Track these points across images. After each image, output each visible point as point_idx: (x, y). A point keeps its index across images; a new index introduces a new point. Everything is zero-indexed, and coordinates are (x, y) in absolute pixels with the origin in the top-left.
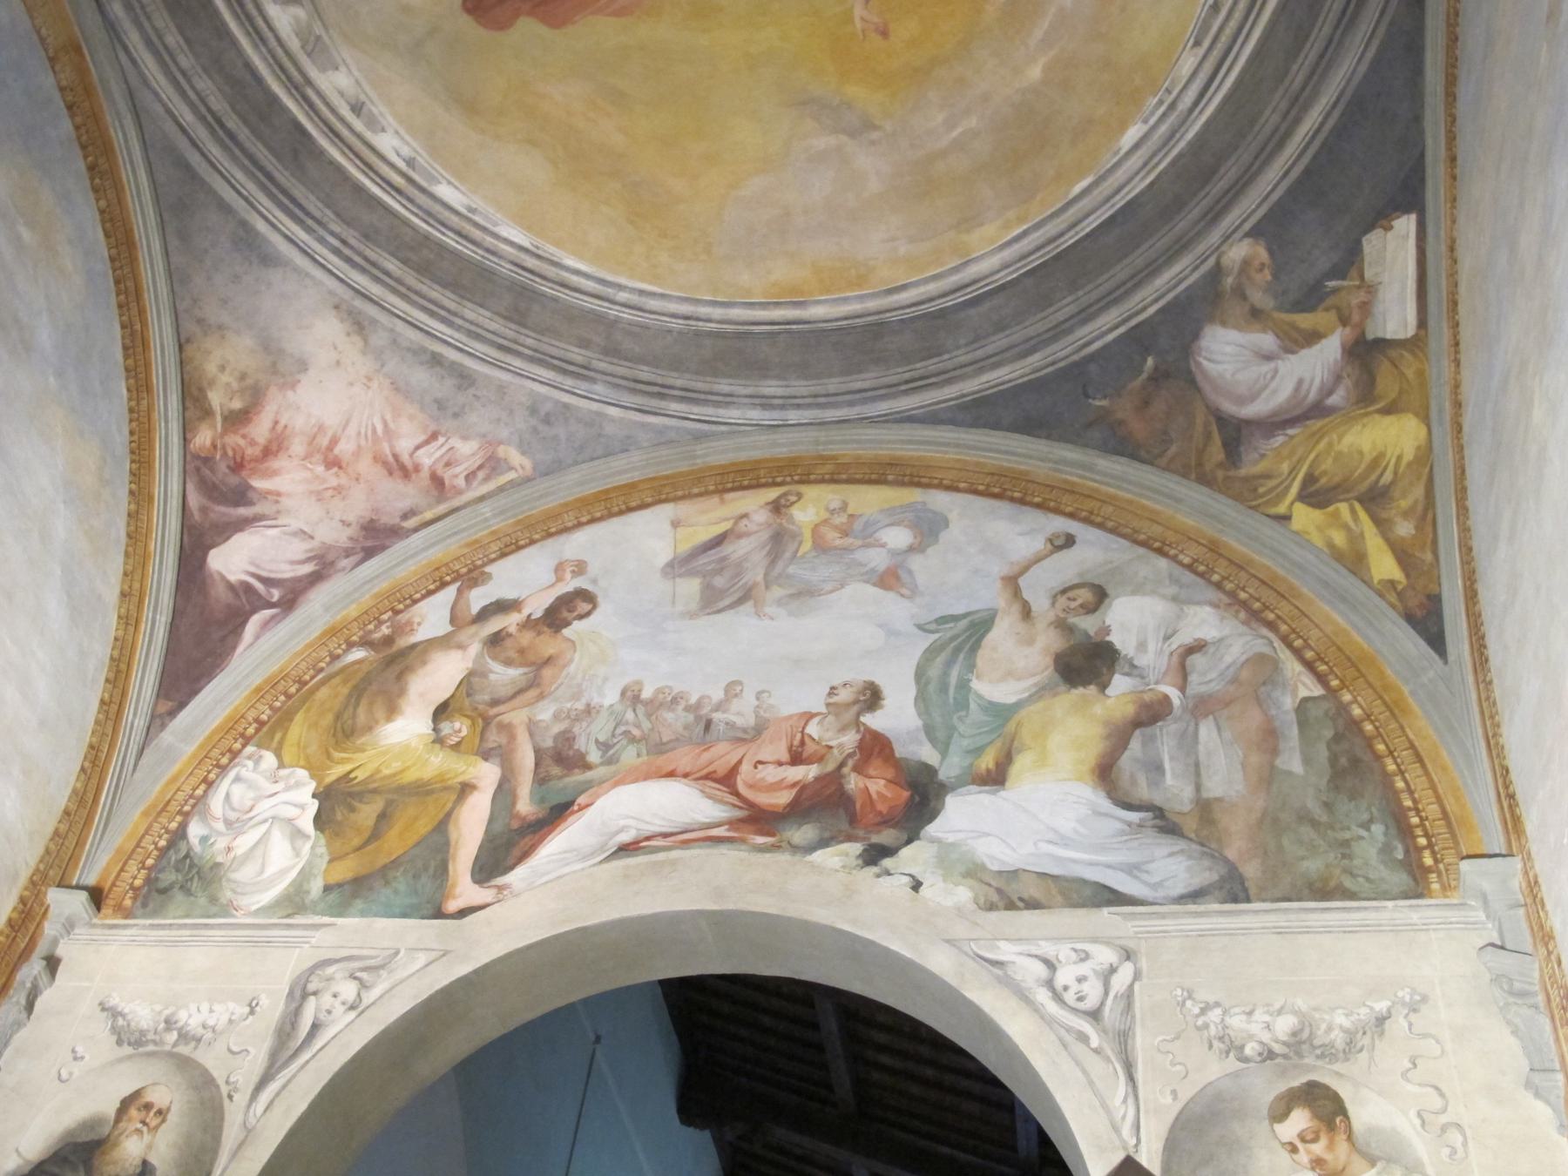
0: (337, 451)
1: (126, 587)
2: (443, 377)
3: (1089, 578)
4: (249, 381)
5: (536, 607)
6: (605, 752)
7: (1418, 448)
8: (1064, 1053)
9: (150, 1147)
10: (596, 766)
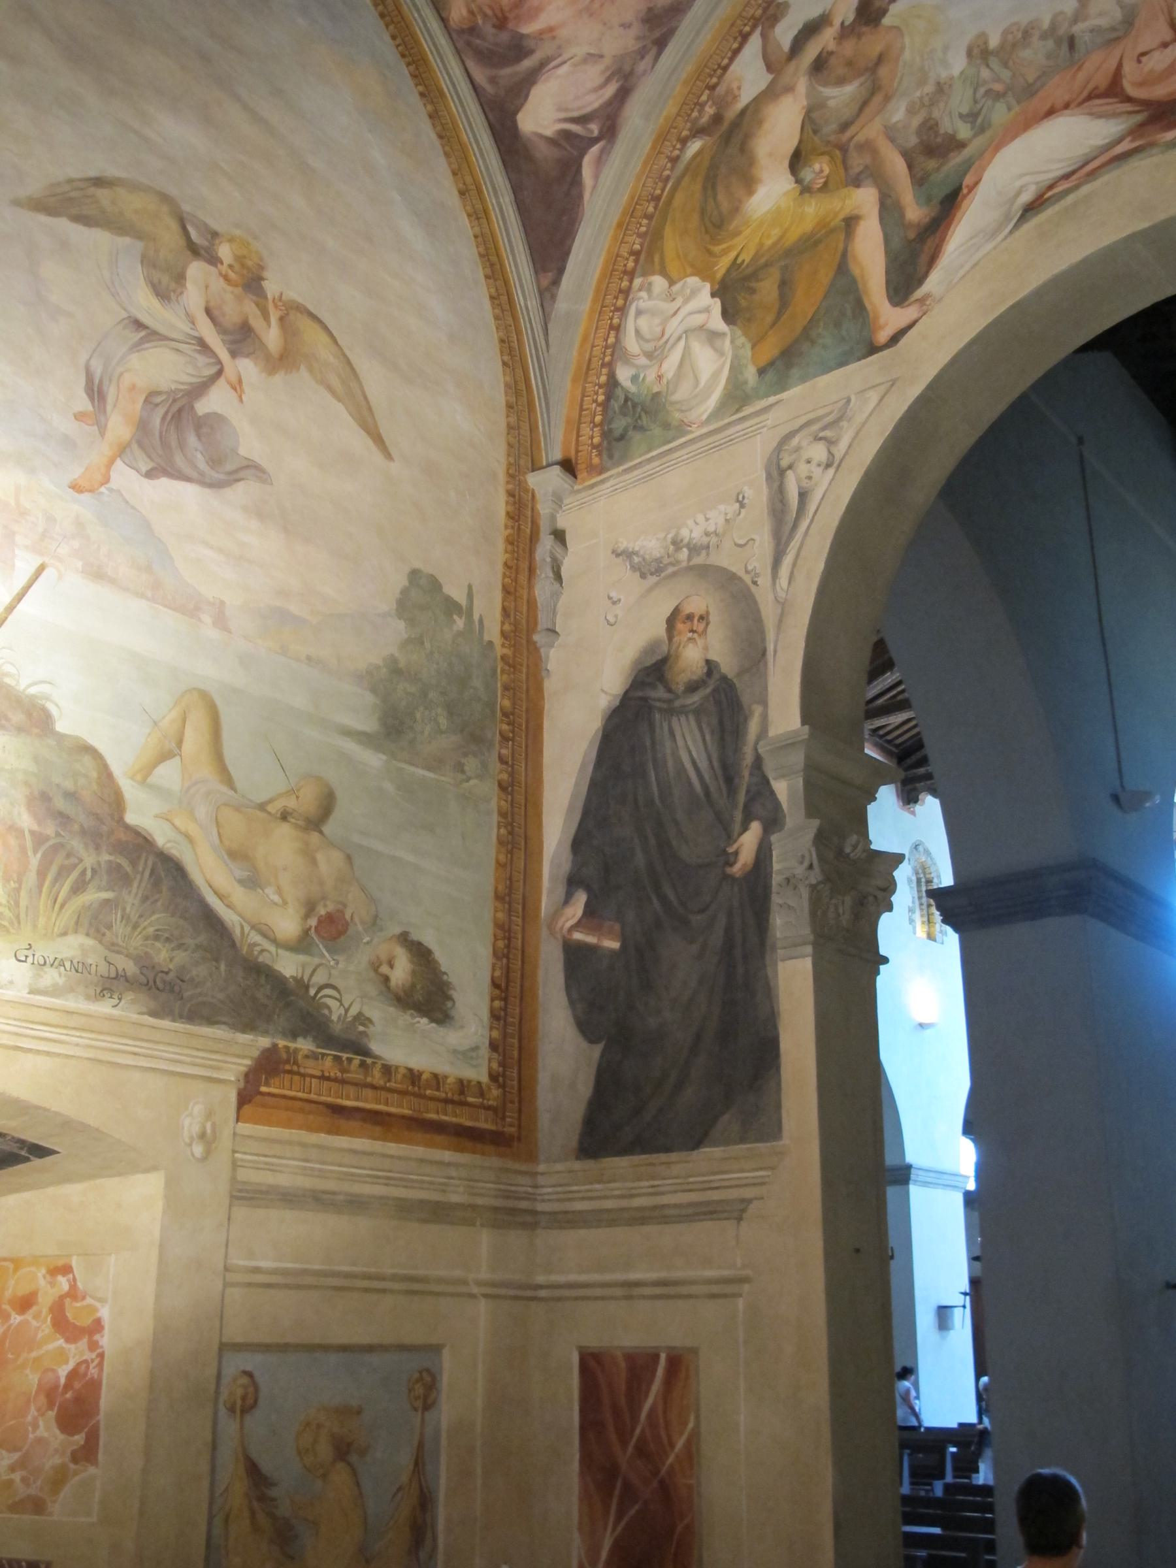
1: (461, 185)
6: (973, 123)
9: (706, 648)
10: (970, 140)
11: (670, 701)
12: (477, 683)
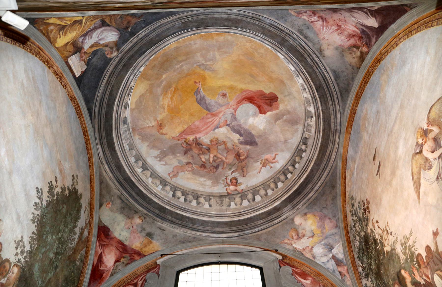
0: (337, 28)
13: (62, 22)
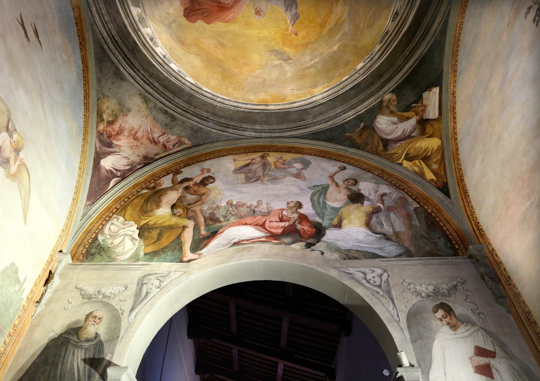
0: (137, 135)
2: (168, 117)
3: (351, 177)
4: (114, 113)
5: (198, 179)
6: (225, 218)
7: (438, 146)
8: (374, 296)
10: (223, 222)
11: (77, 342)
12: (12, 311)
13: (423, 168)
